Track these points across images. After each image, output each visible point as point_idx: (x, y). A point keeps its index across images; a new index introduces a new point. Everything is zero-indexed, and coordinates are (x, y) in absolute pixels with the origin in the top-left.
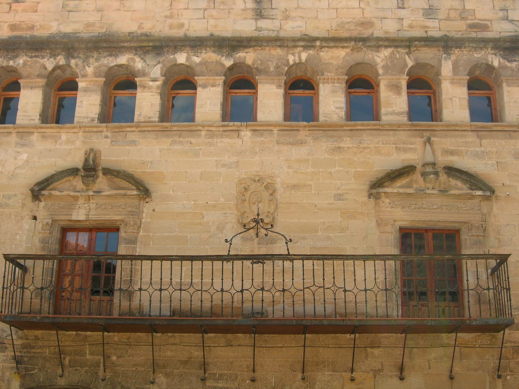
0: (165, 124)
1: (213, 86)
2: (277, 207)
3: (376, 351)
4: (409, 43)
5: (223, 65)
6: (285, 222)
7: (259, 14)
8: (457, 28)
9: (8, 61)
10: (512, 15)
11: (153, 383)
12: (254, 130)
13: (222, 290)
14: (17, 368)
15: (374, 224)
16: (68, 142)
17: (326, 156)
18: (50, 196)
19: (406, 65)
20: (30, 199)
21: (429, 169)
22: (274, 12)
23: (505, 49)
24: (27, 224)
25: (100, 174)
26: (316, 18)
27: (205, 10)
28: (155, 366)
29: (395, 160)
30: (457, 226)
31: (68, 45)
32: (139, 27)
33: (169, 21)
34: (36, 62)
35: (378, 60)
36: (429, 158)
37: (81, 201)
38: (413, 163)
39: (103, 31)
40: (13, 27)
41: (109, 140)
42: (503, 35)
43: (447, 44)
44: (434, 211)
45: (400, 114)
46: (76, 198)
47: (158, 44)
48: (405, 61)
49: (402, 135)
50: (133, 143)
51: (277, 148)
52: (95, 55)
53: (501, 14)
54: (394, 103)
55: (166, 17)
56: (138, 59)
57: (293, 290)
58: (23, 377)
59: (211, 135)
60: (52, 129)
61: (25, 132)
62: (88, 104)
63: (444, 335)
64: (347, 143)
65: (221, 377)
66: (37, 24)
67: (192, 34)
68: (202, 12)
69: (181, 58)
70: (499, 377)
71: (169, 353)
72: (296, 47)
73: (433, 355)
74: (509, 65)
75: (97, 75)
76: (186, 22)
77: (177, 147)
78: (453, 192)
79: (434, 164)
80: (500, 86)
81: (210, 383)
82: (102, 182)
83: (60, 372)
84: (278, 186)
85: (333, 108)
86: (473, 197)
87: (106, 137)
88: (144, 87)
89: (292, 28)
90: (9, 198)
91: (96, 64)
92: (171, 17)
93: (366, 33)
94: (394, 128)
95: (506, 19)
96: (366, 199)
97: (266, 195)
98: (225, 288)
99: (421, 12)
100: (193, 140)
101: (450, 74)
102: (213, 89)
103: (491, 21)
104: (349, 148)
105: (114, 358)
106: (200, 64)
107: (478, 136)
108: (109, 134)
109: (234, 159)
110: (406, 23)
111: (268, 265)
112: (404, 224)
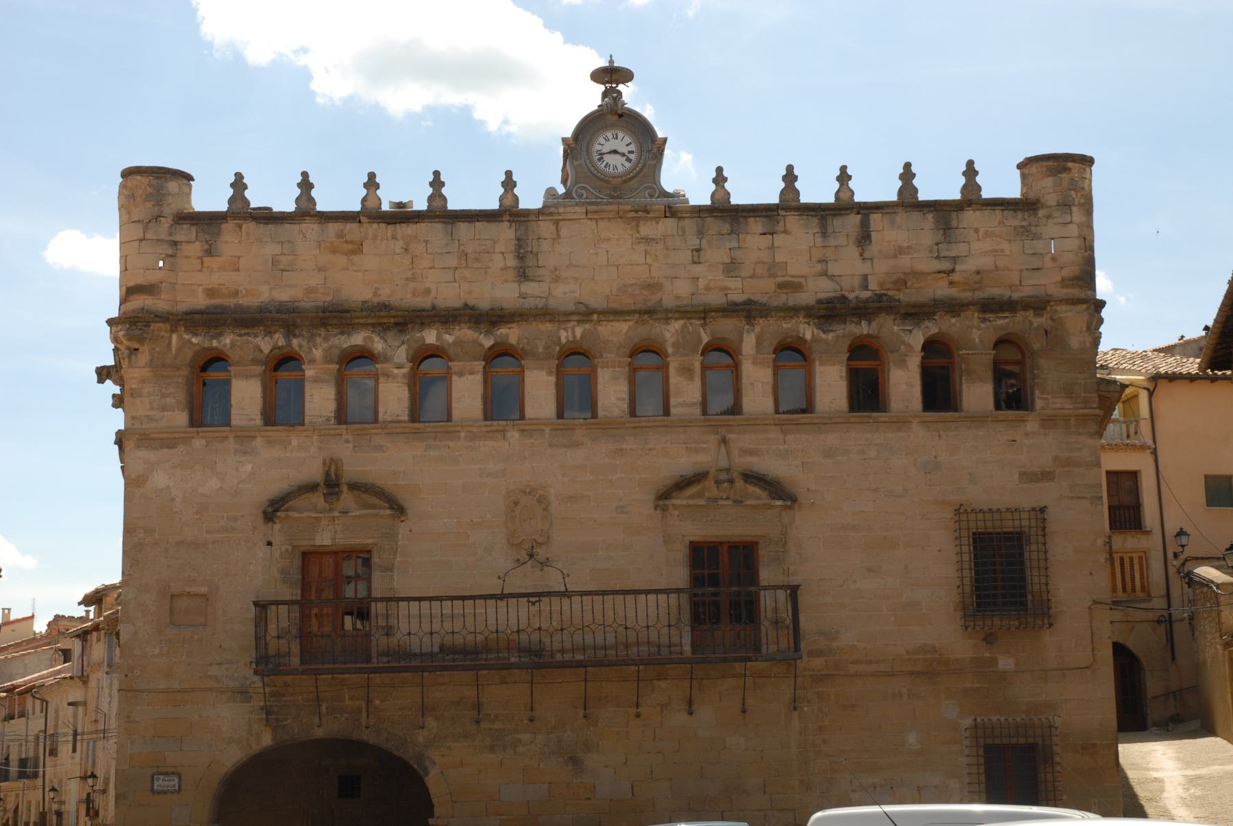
0: (417, 425)
1: (471, 373)
3: (663, 684)
4: (705, 313)
5: (481, 345)
8: (763, 290)
9: (210, 341)
10: (833, 269)
11: (422, 728)
12: (523, 430)
13: (497, 632)
14: (267, 720)
18: (287, 517)
19: (700, 340)
20: (260, 520)
21: (723, 476)
22: (542, 272)
23: (820, 317)
24: (262, 551)
25: (345, 488)
26: (593, 279)
27: (456, 268)
28: (424, 709)
30: (755, 539)
31: (284, 318)
32: (375, 294)
33: (412, 285)
34: (248, 342)
35: (668, 335)
37: (324, 522)
39: (329, 299)
40: (211, 292)
41: (351, 445)
43: (748, 311)
45: (694, 404)
46: (318, 520)
47: (401, 320)
50: (380, 448)
52: (323, 332)
53: (819, 267)
55: (407, 279)
56: (377, 339)
58: (274, 729)
60: (277, 433)
61: (245, 436)
62: (320, 400)
66: (241, 288)
68: (451, 272)
69: (430, 337)
70: (795, 709)
74: (823, 336)
75: (327, 359)
76: (433, 287)
78: (749, 502)
79: (728, 470)
81: (484, 725)
82: (347, 498)
83: (316, 720)
85: (613, 399)
87: (347, 441)
88: (388, 376)
89: (564, 294)
91: (325, 345)
92: (413, 279)
93: (655, 297)
94: (685, 424)
95: (825, 274)
96: (652, 510)
98: (500, 629)
99: (721, 267)
100: (452, 444)
102: (472, 377)
103: (805, 277)
105: (377, 702)
106: (454, 343)
107: (782, 431)
108: (350, 438)
110: (702, 283)
111: (545, 600)
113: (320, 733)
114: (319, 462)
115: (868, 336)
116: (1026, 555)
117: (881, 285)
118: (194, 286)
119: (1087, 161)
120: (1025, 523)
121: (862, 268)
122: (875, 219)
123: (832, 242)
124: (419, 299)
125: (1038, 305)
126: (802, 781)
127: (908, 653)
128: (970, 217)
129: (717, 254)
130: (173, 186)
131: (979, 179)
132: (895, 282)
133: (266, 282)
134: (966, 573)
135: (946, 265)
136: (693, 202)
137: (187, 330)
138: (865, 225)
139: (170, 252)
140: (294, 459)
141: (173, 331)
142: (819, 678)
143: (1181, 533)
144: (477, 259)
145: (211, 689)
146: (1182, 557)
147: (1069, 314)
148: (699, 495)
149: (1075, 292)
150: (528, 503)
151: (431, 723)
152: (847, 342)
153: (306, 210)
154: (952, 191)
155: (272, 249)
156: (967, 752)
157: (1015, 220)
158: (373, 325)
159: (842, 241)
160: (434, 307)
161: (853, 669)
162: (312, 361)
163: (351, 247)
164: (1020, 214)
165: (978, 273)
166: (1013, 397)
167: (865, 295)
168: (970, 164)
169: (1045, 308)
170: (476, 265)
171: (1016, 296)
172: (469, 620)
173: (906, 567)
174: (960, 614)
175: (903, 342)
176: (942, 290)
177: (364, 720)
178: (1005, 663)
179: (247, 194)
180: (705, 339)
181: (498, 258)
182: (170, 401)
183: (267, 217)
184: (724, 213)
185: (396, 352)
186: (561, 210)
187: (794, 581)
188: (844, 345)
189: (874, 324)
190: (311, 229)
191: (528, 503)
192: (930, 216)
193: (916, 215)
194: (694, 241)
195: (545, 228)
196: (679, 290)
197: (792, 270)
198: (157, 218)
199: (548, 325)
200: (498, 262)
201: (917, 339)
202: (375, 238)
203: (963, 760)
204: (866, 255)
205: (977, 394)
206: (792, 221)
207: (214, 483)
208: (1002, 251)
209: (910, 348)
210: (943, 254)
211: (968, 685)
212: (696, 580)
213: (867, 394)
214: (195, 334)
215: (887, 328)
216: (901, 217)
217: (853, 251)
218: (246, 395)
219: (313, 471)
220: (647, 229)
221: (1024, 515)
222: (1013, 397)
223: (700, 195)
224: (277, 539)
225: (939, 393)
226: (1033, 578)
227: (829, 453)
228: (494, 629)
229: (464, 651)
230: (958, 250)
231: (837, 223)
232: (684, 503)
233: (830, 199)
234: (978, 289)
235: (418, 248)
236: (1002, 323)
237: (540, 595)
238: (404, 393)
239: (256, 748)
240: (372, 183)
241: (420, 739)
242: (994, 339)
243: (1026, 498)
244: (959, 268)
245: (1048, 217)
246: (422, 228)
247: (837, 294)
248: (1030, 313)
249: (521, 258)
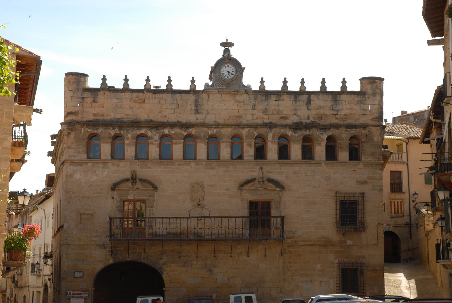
0: (161, 160)
1: (180, 144)
3: (240, 247)
4: (256, 126)
5: (183, 135)
7: (197, 112)
8: (275, 119)
10: (298, 113)
19: (254, 135)
20: (110, 190)
21: (261, 180)
23: (293, 128)
24: (110, 200)
25: (138, 180)
29: (248, 175)
31: (118, 124)
32: (149, 117)
33: (160, 114)
34: (107, 131)
35: (244, 133)
40: (94, 115)
41: (140, 166)
43: (270, 126)
45: (251, 156)
46: (129, 190)
47: (157, 126)
48: (254, 133)
50: (149, 167)
52: (131, 129)
53: (294, 112)
54: (249, 152)
55: (159, 112)
56: (149, 132)
58: (114, 258)
60: (115, 162)
61: (105, 162)
62: (130, 151)
64: (231, 168)
69: (166, 131)
70: (282, 256)
75: (133, 138)
76: (168, 115)
77: (166, 170)
79: (262, 178)
82: (138, 183)
83: (127, 256)
84: (205, 185)
86: (276, 190)
87: (139, 165)
89: (210, 119)
92: (161, 112)
93: (239, 121)
94: (249, 162)
95: (295, 114)
96: (237, 190)
99: (262, 111)
100: (172, 167)
101: (271, 139)
102: (179, 145)
103: (289, 115)
106: (174, 134)
107: (280, 166)
108: (140, 164)
110: (255, 116)
111: (203, 219)
112: (250, 200)
113: (128, 259)
115: (309, 135)
116: (357, 208)
117: (314, 118)
119: (382, 80)
120: (357, 198)
122: (313, 96)
123: (298, 104)
124: (163, 119)
125: (364, 126)
127: (318, 238)
128: (343, 97)
129: (261, 107)
130: (82, 79)
131: (346, 84)
132: (318, 118)
133: (113, 112)
134: (338, 213)
135: (335, 112)
136: (253, 89)
137: (87, 127)
138: (309, 98)
140: (122, 171)
141: (82, 127)
142: (289, 246)
143: (415, 194)
144: (182, 106)
145: (93, 245)
146: (415, 202)
147: (374, 130)
149: (376, 123)
150: (197, 187)
152: (302, 137)
154: (338, 88)
155: (115, 101)
156: (336, 271)
157: (358, 98)
158: (148, 127)
159: (302, 103)
160: (168, 122)
161: (300, 243)
162: (128, 138)
163: (141, 101)
164: (359, 96)
165: (345, 115)
167: (308, 121)
168: (344, 79)
170: (182, 108)
171: (357, 123)
172: (179, 224)
174: (335, 226)
175: (320, 137)
176: (333, 121)
178: (349, 242)
179: (107, 82)
180: (256, 134)
181: (189, 106)
182: (81, 150)
183: (112, 90)
184: (263, 93)
185: (155, 136)
186: (210, 91)
187: (283, 214)
189: (311, 131)
190: (128, 94)
191: (197, 187)
192: (330, 96)
193: (326, 96)
194: (253, 102)
195: (205, 96)
196: (247, 119)
198: (77, 90)
200: (189, 107)
201: (325, 137)
202: (149, 98)
203: (335, 273)
204: (309, 108)
205: (343, 155)
206: (285, 96)
207: (95, 178)
208: (353, 108)
209: (322, 139)
210: (334, 109)
212: (251, 214)
213: (308, 154)
214: (89, 128)
215: (315, 132)
216: (321, 96)
217: (305, 107)
218: (106, 149)
219: (128, 175)
220: (238, 98)
221: (357, 195)
224: (115, 196)
225: (331, 154)
226: (359, 215)
227: (295, 173)
228: (186, 228)
229: (176, 235)
230: (339, 107)
231: (300, 97)
235: (163, 102)
236: (353, 132)
237: (202, 217)
238: (157, 149)
239: (108, 264)
240: (148, 80)
241: (161, 262)
242: (350, 137)
243: (358, 189)
244: (339, 113)
245: (369, 98)
246: (164, 95)
247: (299, 121)
248: (362, 129)
249: (196, 106)
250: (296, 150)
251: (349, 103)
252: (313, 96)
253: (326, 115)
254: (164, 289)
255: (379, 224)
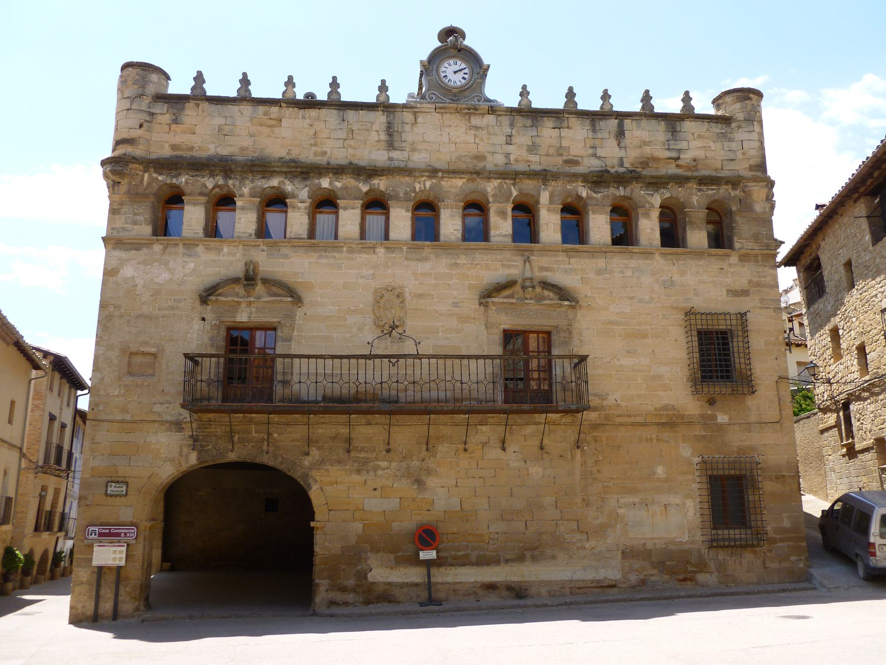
1: (353, 208)
2: (406, 313)
3: (484, 428)
4: (515, 176)
5: (360, 190)
6: (412, 326)
8: (555, 163)
9: (171, 179)
10: (600, 152)
12: (387, 248)
13: (366, 383)
14: (194, 445)
15: (483, 327)
16: (229, 254)
17: (446, 271)
18: (217, 301)
19: (511, 195)
20: (198, 303)
21: (528, 283)
22: (404, 144)
24: (197, 325)
25: (259, 283)
28: (309, 442)
31: (223, 166)
32: (288, 154)
33: (314, 149)
34: (198, 181)
35: (489, 189)
36: (528, 274)
37: (243, 305)
38: (515, 278)
39: (257, 155)
40: (174, 147)
41: (265, 253)
42: (592, 169)
43: (544, 176)
44: (530, 315)
46: (239, 303)
47: (305, 170)
49: (507, 254)
50: (286, 256)
51: (405, 263)
53: (590, 151)
54: (502, 226)
55: (311, 145)
56: (287, 182)
57: (421, 382)
58: (199, 452)
59: (351, 251)
60: (213, 242)
63: (536, 415)
64: (463, 260)
65: (362, 450)
66: (195, 145)
67: (334, 162)
68: (342, 141)
69: (325, 183)
70: (578, 447)
71: (320, 431)
72: (422, 176)
73: (528, 431)
74: (595, 195)
75: (253, 195)
76: (329, 151)
77: (324, 261)
80: (587, 213)
81: (353, 454)
82: (260, 288)
83: (230, 447)
84: (407, 295)
86: (561, 306)
87: (263, 251)
88: (294, 207)
89: (419, 159)
90: (180, 301)
93: (480, 165)
95: (594, 155)
96: (477, 306)
97: (397, 301)
99: (525, 148)
100: (336, 255)
101: (547, 202)
102: (352, 211)
104: (464, 264)
105: (276, 435)
106: (342, 188)
108: (265, 248)
109: (371, 272)
110: (512, 157)
111: (402, 361)
112: (507, 327)
114: (243, 263)
115: (625, 198)
117: (632, 165)
118: (163, 140)
121: (617, 153)
122: (627, 122)
123: (600, 136)
124: (319, 158)
125: (735, 182)
126: (584, 499)
127: (656, 410)
128: (688, 126)
130: (154, 77)
131: (693, 103)
132: (641, 163)
133: (213, 142)
135: (674, 154)
138: (621, 126)
139: (148, 118)
140: (226, 261)
141: (146, 172)
142: (595, 426)
145: (154, 421)
147: (756, 188)
148: (511, 296)
150: (388, 297)
151: (315, 453)
153: (244, 98)
155: (219, 121)
156: (698, 480)
157: (717, 129)
158: (286, 173)
159: (606, 135)
161: (618, 420)
162: (242, 196)
164: (720, 125)
166: (720, 240)
167: (621, 170)
169: (739, 184)
173: (653, 351)
175: (647, 202)
176: (672, 170)
177: (265, 447)
178: (722, 418)
180: (515, 193)
184: (528, 114)
186: (419, 105)
188: (609, 202)
190: (247, 109)
191: (388, 297)
193: (653, 122)
194: (508, 130)
197: (572, 152)
198: (141, 96)
199: (407, 178)
201: (657, 200)
203: (695, 486)
204: (622, 145)
205: (697, 237)
206: (573, 121)
207: (166, 276)
208: (710, 147)
209: (653, 206)
211: (697, 433)
214: (160, 174)
215: (638, 192)
216: (644, 123)
217: (614, 143)
219: (238, 270)
220: (476, 121)
221: (733, 317)
222: (720, 240)
223: (512, 101)
224: (209, 316)
225: (671, 237)
226: (738, 361)
229: (340, 400)
230: (683, 145)
231: (602, 124)
232: (501, 300)
233: (597, 108)
234: (696, 171)
236: (711, 192)
237: (399, 357)
239: (185, 467)
241: (306, 463)
243: (734, 306)
245: (739, 127)
246: (324, 112)
247: (604, 169)
250: (600, 227)
251: (700, 136)
252: (627, 122)
253: (656, 159)
254: (312, 524)
255: (780, 378)
